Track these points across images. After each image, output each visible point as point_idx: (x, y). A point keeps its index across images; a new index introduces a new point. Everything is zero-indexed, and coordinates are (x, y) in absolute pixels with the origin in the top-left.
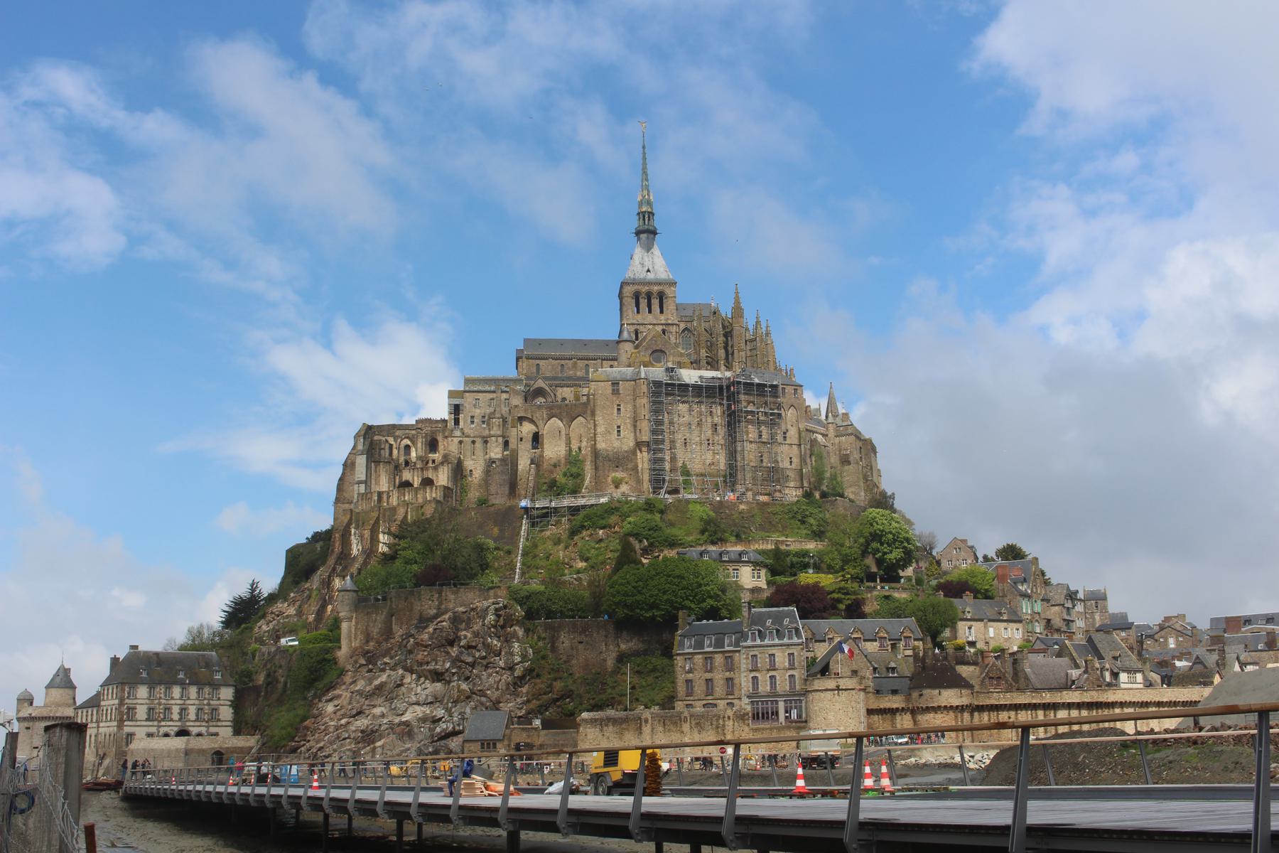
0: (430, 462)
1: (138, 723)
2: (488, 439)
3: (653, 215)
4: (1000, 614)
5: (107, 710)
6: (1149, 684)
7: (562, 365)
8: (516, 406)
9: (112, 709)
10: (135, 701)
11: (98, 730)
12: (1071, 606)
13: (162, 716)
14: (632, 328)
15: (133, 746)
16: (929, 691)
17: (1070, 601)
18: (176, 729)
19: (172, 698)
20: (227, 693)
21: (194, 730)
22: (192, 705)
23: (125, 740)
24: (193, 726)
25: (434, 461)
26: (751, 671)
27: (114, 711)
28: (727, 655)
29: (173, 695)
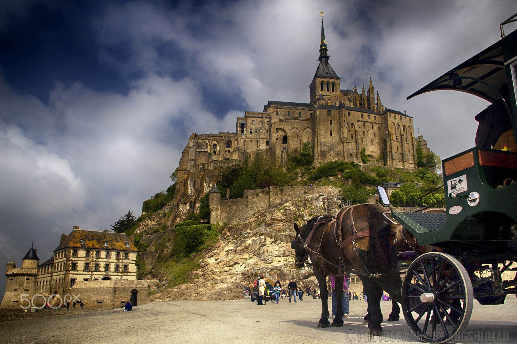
0: (227, 152)
1: (79, 272)
2: (259, 140)
5: (58, 265)
9: (61, 264)
11: (52, 278)
13: (94, 268)
15: (75, 286)
18: (102, 277)
20: (133, 256)
22: (112, 262)
23: (70, 283)
24: (113, 275)
25: (229, 151)
27: (63, 265)
29: (101, 256)
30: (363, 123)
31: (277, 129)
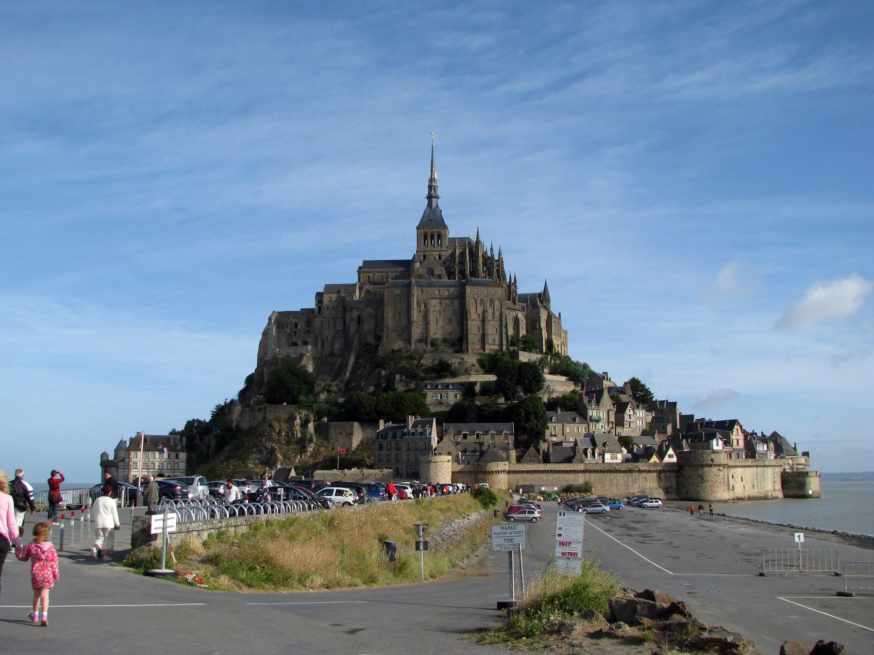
2: (336, 319)
3: (437, 187)
4: (574, 420)
6: (627, 461)
7: (382, 276)
8: (349, 302)
10: (137, 460)
12: (632, 412)
14: (422, 254)
16: (481, 463)
17: (632, 411)
18: (157, 473)
19: (155, 458)
21: (166, 474)
25: (309, 332)
26: (408, 451)
28: (397, 442)
30: (438, 300)
31: (352, 308)
